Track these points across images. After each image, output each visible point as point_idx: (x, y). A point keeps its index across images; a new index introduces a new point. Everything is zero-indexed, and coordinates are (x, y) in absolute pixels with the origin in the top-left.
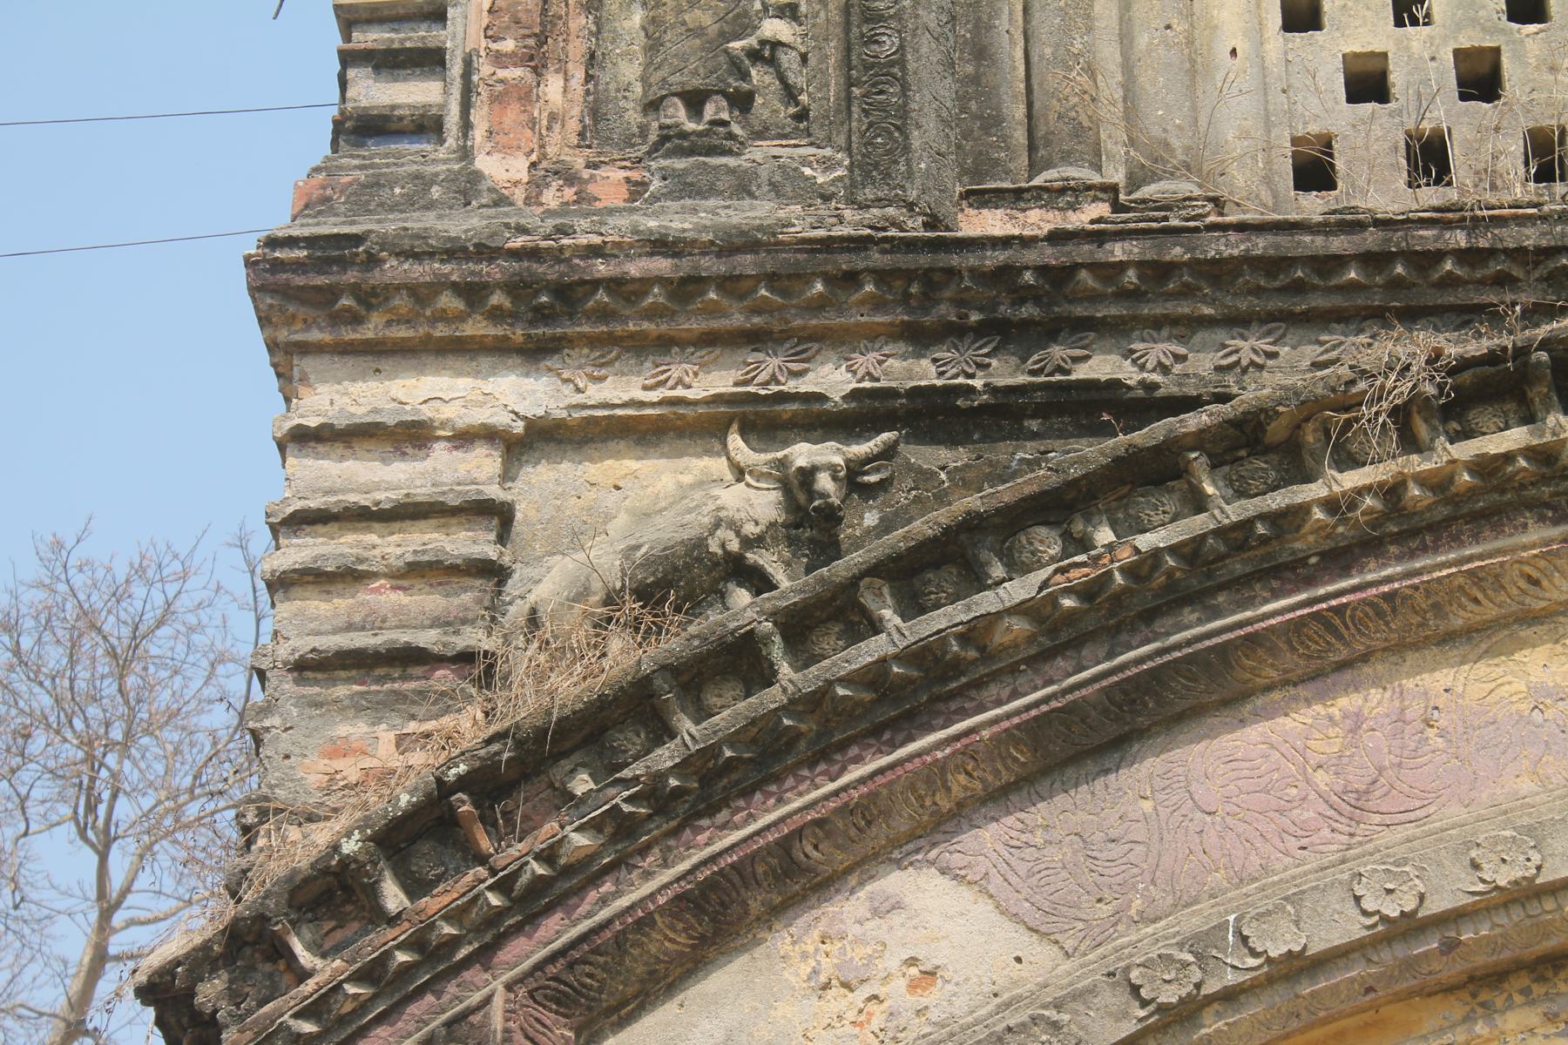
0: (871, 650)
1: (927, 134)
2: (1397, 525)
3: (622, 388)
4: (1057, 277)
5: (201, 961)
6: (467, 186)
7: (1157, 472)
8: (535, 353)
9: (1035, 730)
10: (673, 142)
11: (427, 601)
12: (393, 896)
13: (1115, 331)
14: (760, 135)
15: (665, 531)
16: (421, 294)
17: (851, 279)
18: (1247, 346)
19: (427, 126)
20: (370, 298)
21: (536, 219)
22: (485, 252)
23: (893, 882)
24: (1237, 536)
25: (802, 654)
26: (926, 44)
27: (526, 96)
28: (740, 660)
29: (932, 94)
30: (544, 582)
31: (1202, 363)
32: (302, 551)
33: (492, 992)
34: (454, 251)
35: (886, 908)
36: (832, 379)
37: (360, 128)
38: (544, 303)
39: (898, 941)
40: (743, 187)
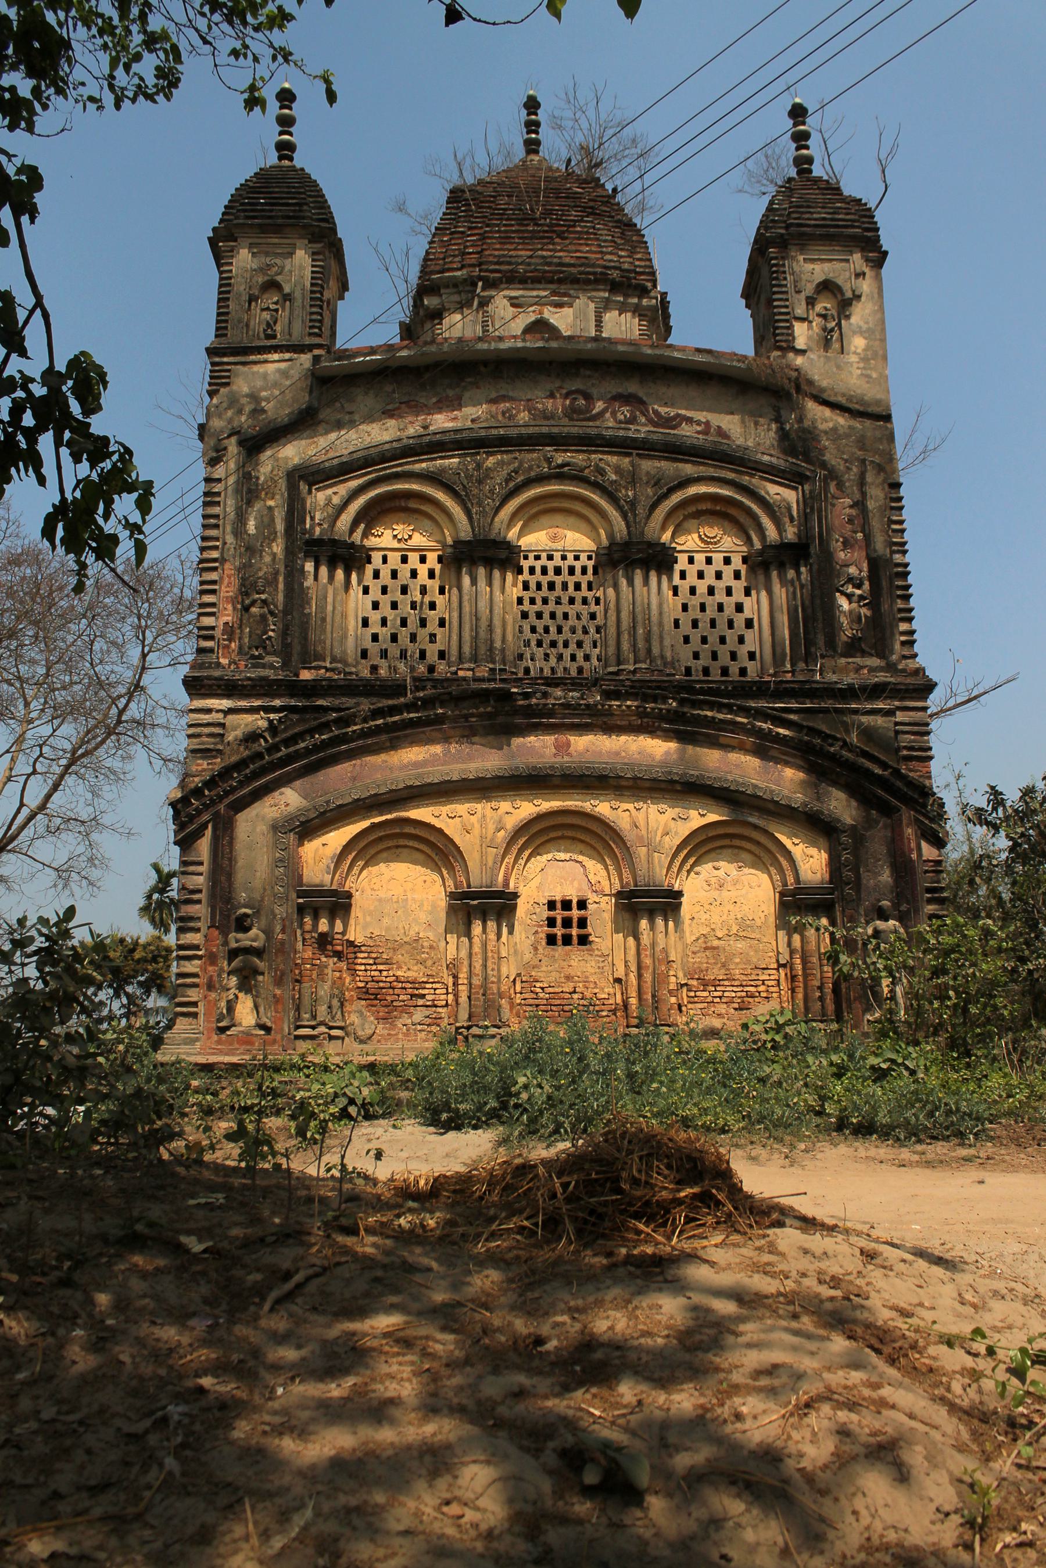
0: (279, 755)
1: (295, 657)
2: (364, 734)
3: (243, 703)
4: (314, 687)
5: (178, 801)
6: (218, 665)
7: (325, 727)
8: (228, 696)
9: (305, 766)
10: (253, 657)
11: (212, 740)
12: (207, 792)
13: (323, 696)
14: (268, 654)
15: (250, 729)
16: (210, 686)
17: (279, 686)
18: (344, 699)
19: (211, 650)
20: (203, 686)
21: (228, 675)
22: (220, 679)
23: (283, 790)
24: (337, 736)
25: (269, 755)
26: (296, 641)
27: (227, 647)
28: (259, 756)
29: (297, 649)
30: (230, 737)
31: (337, 702)
32: (192, 731)
33: (222, 807)
34: (216, 679)
35: (282, 794)
36: (277, 703)
37: (200, 651)
38: (230, 688)
39: (283, 800)
40: (264, 666)
